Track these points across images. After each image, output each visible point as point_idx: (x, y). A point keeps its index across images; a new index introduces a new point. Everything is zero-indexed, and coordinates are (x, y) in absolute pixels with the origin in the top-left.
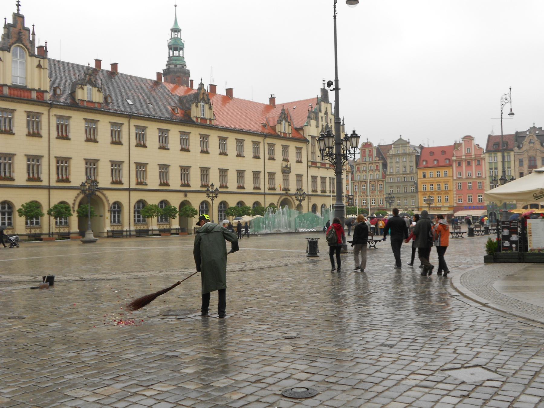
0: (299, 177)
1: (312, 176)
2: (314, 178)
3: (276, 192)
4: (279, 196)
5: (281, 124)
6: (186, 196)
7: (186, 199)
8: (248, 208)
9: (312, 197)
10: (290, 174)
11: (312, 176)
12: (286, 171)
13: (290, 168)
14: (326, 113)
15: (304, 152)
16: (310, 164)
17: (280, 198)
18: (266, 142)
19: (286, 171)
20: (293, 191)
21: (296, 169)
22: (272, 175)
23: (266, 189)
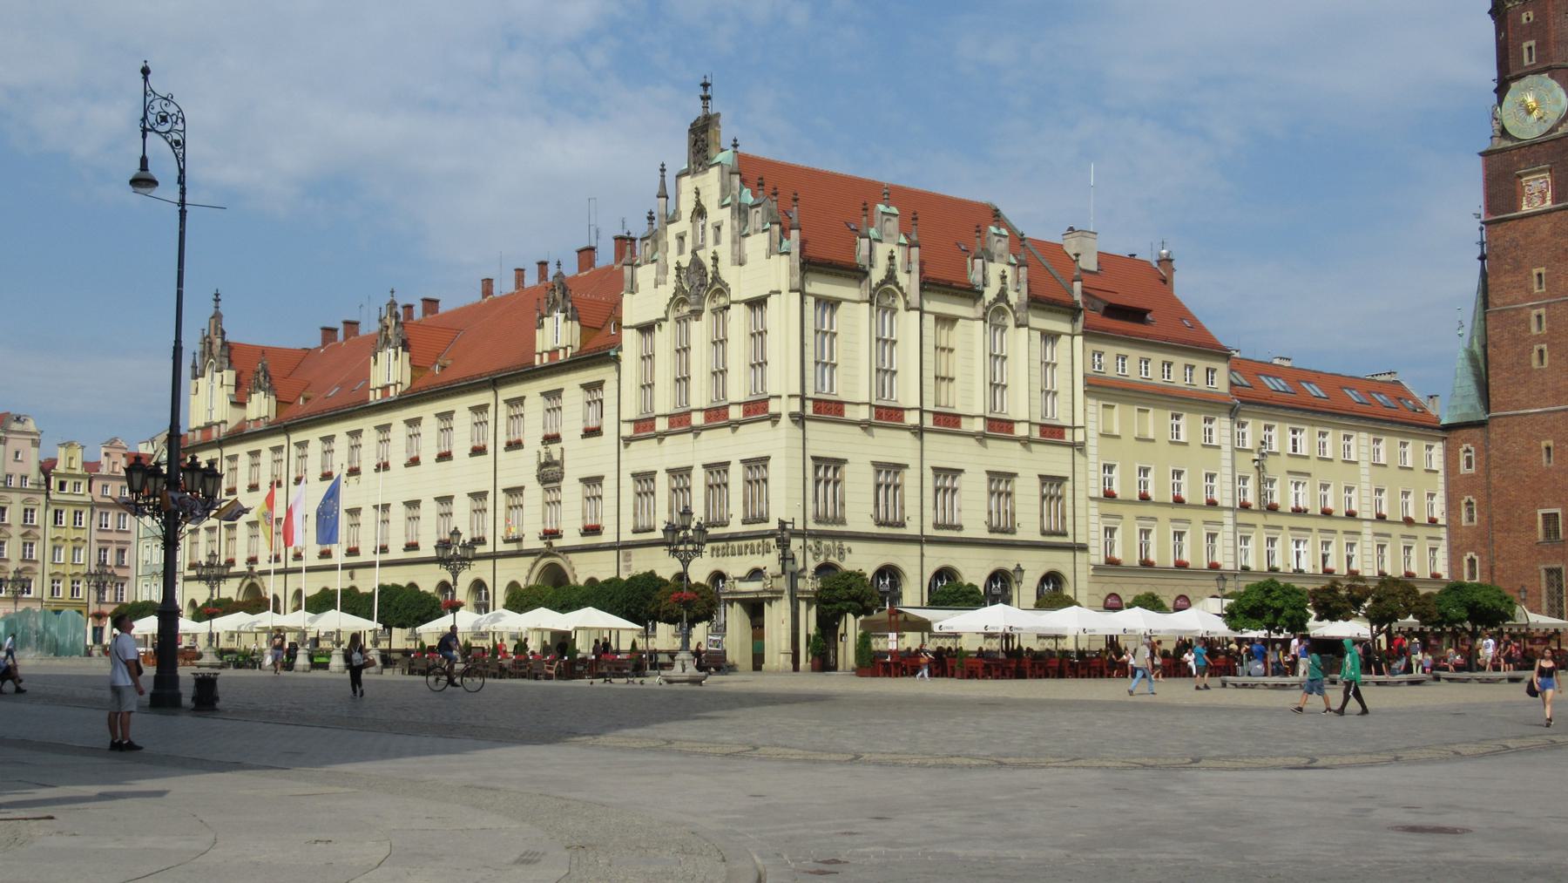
0: (593, 481)
1: (633, 475)
2: (644, 478)
3: (526, 546)
4: (531, 559)
5: (541, 326)
6: (352, 576)
7: (353, 583)
8: (973, 589)
9: (634, 551)
10: (564, 484)
11: (633, 475)
12: (550, 474)
13: (559, 464)
14: (700, 212)
15: (608, 394)
16: (627, 430)
17: (534, 565)
18: (500, 401)
19: (550, 474)
20: (571, 537)
21: (579, 458)
22: (515, 491)
23: (499, 541)
